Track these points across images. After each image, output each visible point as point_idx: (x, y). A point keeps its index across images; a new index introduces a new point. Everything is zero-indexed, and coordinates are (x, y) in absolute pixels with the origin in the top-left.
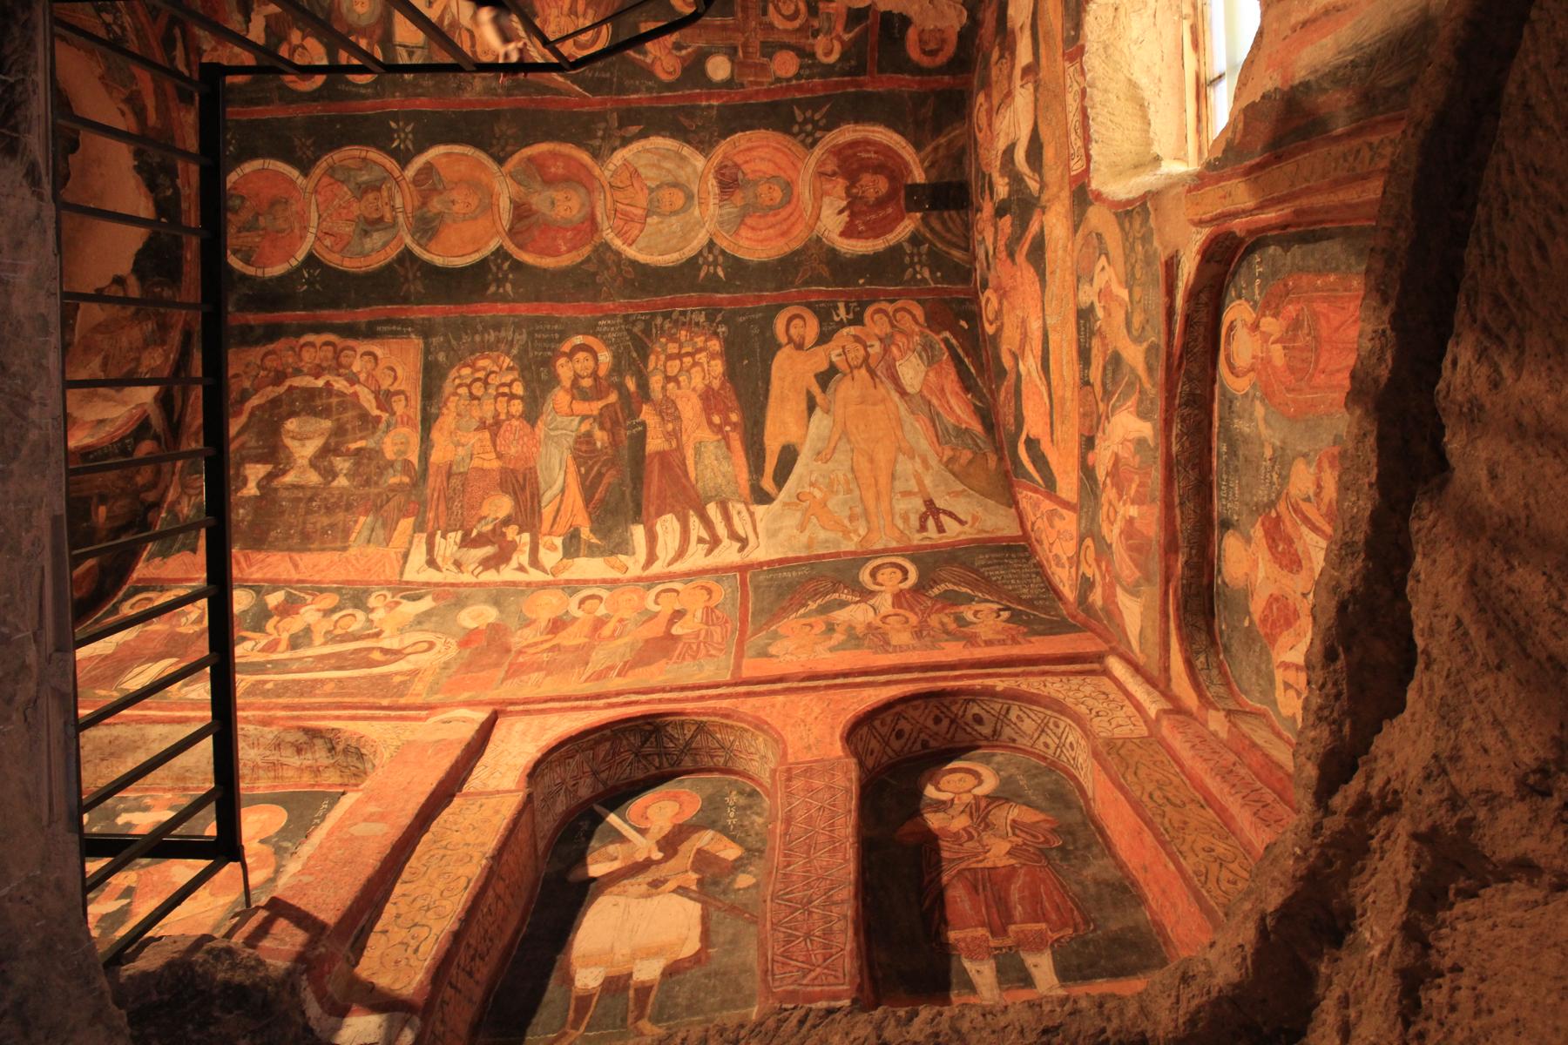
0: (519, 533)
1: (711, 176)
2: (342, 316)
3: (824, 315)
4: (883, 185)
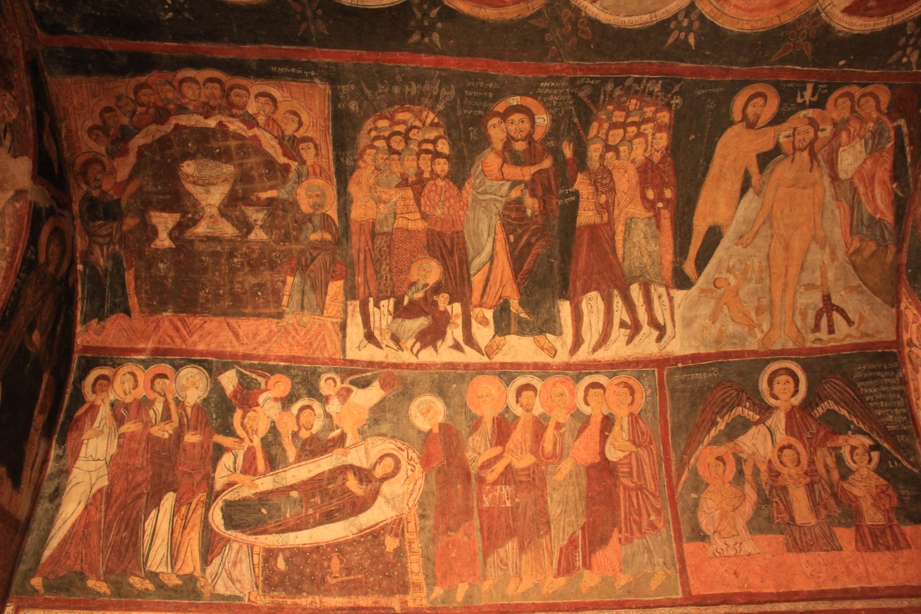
0: (450, 303)
2: (226, 51)
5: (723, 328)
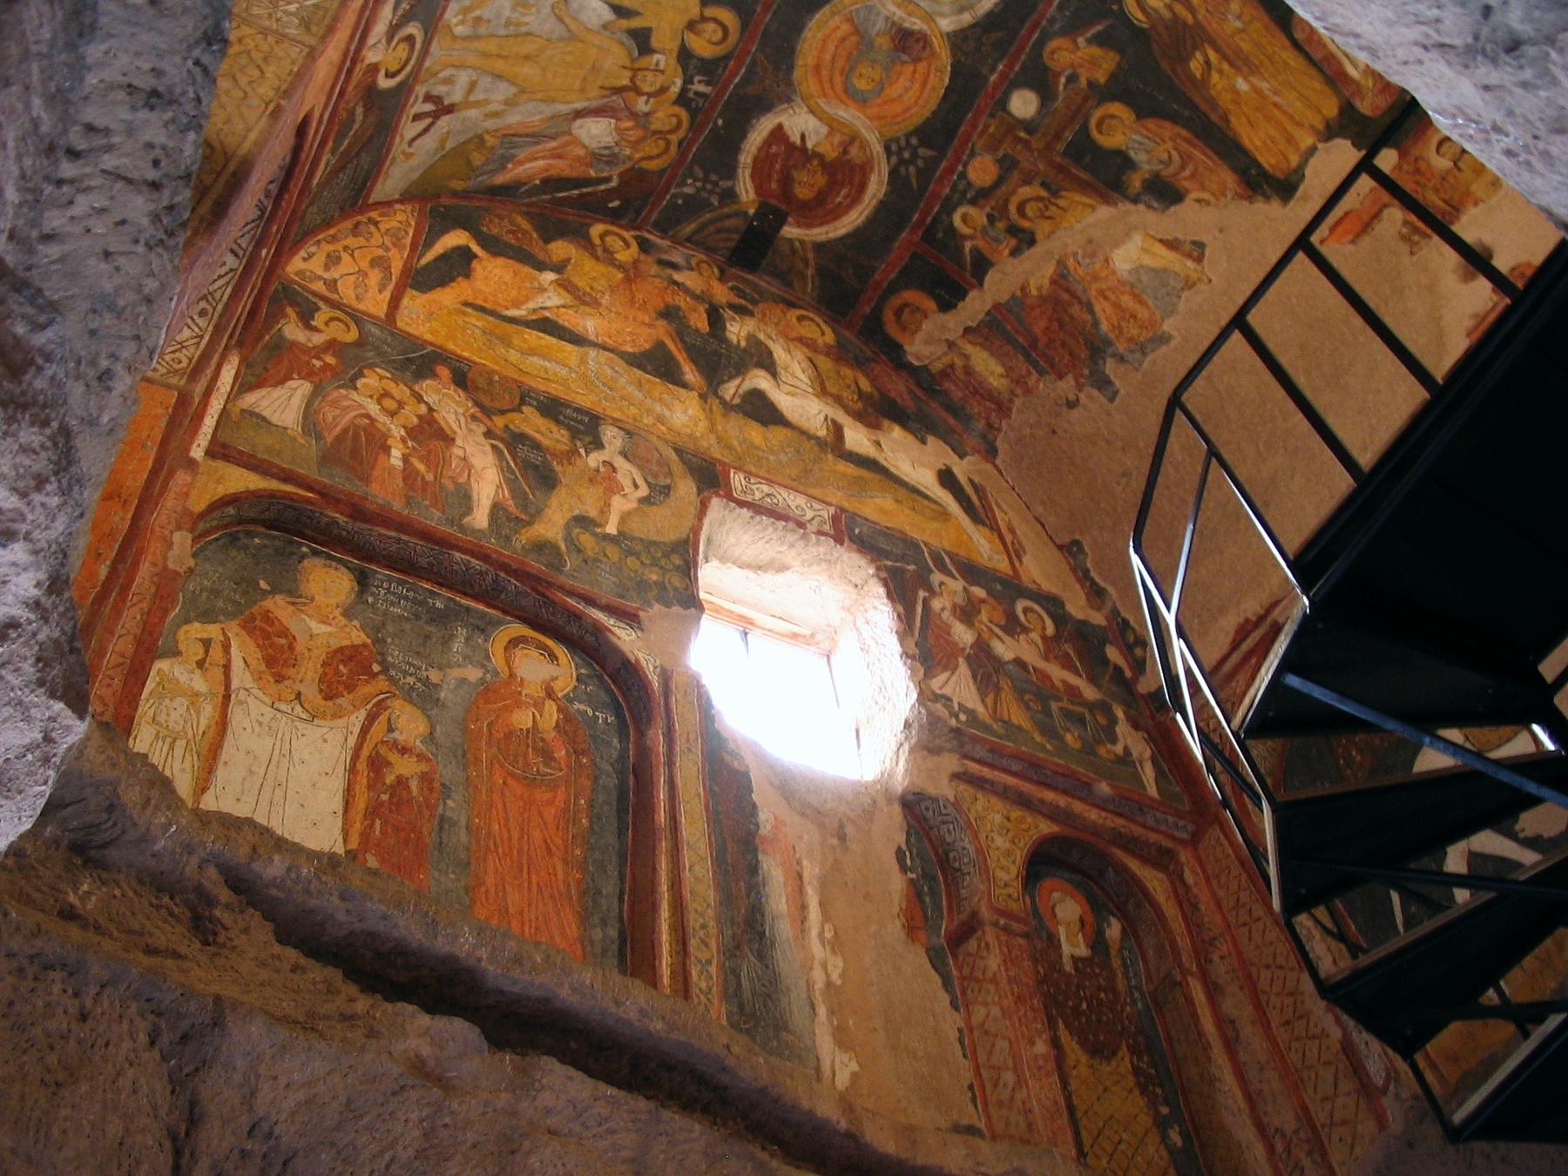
1: (925, 27)
3: (709, 68)
4: (802, 193)
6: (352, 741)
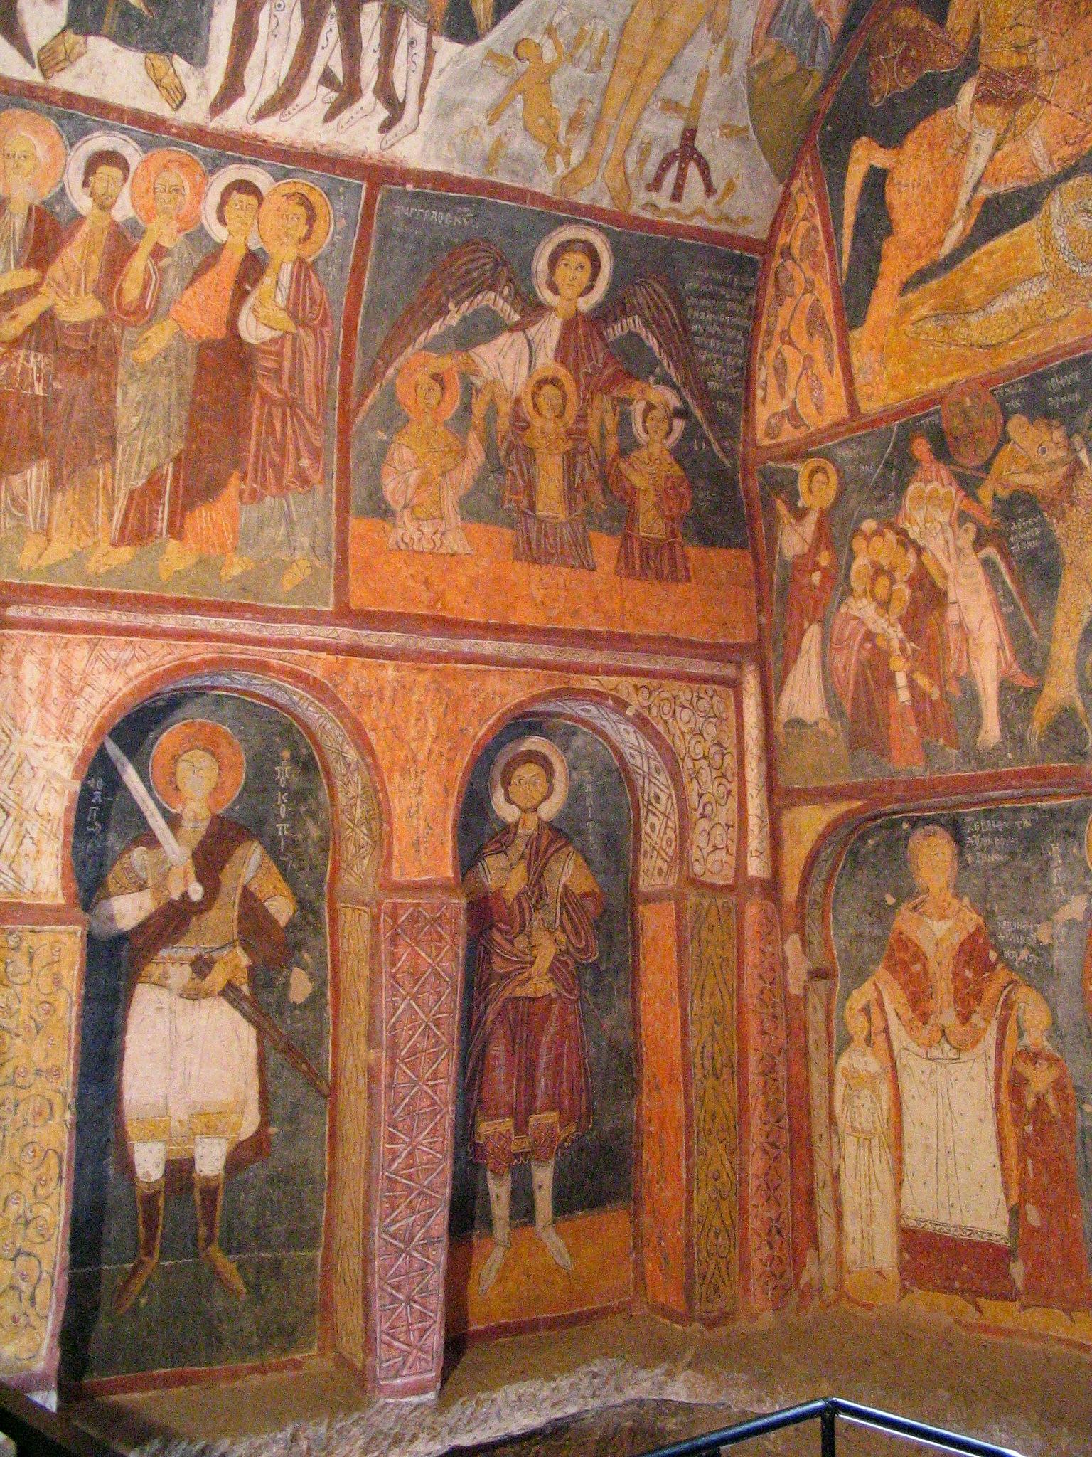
5: (505, 139)
6: (992, 1068)
